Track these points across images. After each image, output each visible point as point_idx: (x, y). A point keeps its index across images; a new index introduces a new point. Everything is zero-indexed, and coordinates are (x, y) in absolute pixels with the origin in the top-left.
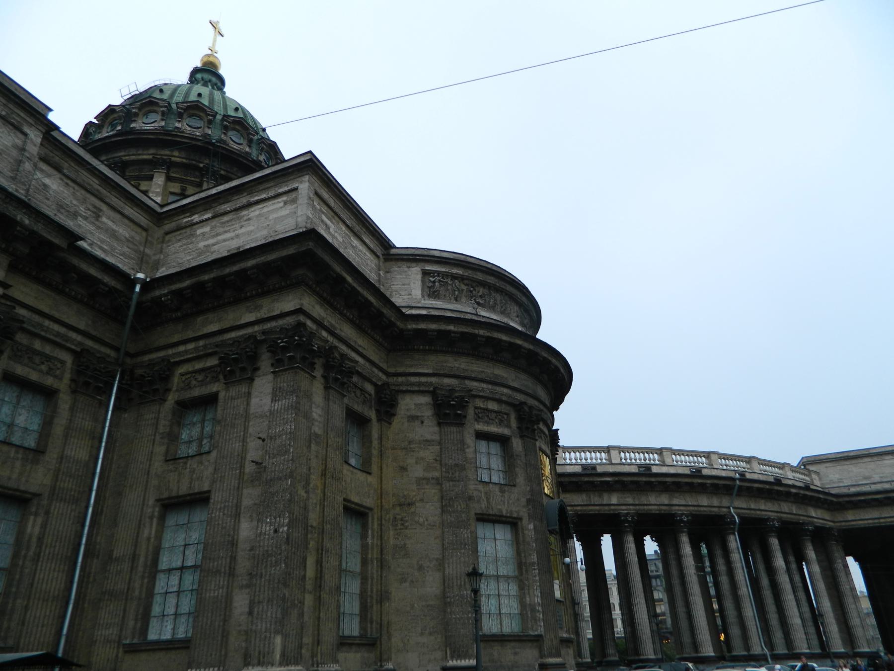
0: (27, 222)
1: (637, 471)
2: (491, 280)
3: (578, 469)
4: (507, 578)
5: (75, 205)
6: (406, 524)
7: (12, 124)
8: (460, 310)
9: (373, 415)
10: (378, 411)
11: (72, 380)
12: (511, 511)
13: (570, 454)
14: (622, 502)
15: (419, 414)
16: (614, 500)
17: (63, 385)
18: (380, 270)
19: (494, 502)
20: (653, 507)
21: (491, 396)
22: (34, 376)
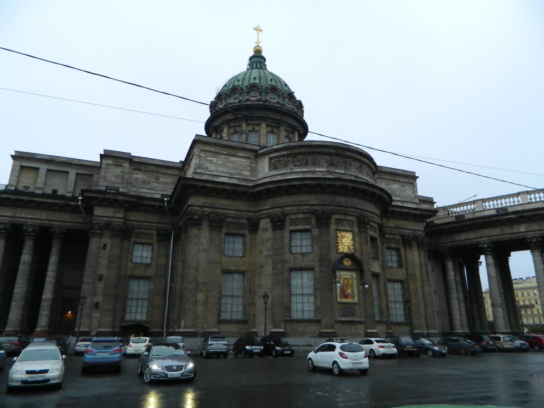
0: (122, 198)
2: (303, 150)
3: (493, 212)
4: (308, 295)
5: (149, 180)
6: (261, 275)
7: (119, 165)
9: (246, 232)
11: (157, 239)
14: (529, 229)
15: (266, 227)
16: (523, 228)
17: (154, 241)
18: (252, 164)
19: (298, 262)
21: (298, 212)
22: (144, 241)
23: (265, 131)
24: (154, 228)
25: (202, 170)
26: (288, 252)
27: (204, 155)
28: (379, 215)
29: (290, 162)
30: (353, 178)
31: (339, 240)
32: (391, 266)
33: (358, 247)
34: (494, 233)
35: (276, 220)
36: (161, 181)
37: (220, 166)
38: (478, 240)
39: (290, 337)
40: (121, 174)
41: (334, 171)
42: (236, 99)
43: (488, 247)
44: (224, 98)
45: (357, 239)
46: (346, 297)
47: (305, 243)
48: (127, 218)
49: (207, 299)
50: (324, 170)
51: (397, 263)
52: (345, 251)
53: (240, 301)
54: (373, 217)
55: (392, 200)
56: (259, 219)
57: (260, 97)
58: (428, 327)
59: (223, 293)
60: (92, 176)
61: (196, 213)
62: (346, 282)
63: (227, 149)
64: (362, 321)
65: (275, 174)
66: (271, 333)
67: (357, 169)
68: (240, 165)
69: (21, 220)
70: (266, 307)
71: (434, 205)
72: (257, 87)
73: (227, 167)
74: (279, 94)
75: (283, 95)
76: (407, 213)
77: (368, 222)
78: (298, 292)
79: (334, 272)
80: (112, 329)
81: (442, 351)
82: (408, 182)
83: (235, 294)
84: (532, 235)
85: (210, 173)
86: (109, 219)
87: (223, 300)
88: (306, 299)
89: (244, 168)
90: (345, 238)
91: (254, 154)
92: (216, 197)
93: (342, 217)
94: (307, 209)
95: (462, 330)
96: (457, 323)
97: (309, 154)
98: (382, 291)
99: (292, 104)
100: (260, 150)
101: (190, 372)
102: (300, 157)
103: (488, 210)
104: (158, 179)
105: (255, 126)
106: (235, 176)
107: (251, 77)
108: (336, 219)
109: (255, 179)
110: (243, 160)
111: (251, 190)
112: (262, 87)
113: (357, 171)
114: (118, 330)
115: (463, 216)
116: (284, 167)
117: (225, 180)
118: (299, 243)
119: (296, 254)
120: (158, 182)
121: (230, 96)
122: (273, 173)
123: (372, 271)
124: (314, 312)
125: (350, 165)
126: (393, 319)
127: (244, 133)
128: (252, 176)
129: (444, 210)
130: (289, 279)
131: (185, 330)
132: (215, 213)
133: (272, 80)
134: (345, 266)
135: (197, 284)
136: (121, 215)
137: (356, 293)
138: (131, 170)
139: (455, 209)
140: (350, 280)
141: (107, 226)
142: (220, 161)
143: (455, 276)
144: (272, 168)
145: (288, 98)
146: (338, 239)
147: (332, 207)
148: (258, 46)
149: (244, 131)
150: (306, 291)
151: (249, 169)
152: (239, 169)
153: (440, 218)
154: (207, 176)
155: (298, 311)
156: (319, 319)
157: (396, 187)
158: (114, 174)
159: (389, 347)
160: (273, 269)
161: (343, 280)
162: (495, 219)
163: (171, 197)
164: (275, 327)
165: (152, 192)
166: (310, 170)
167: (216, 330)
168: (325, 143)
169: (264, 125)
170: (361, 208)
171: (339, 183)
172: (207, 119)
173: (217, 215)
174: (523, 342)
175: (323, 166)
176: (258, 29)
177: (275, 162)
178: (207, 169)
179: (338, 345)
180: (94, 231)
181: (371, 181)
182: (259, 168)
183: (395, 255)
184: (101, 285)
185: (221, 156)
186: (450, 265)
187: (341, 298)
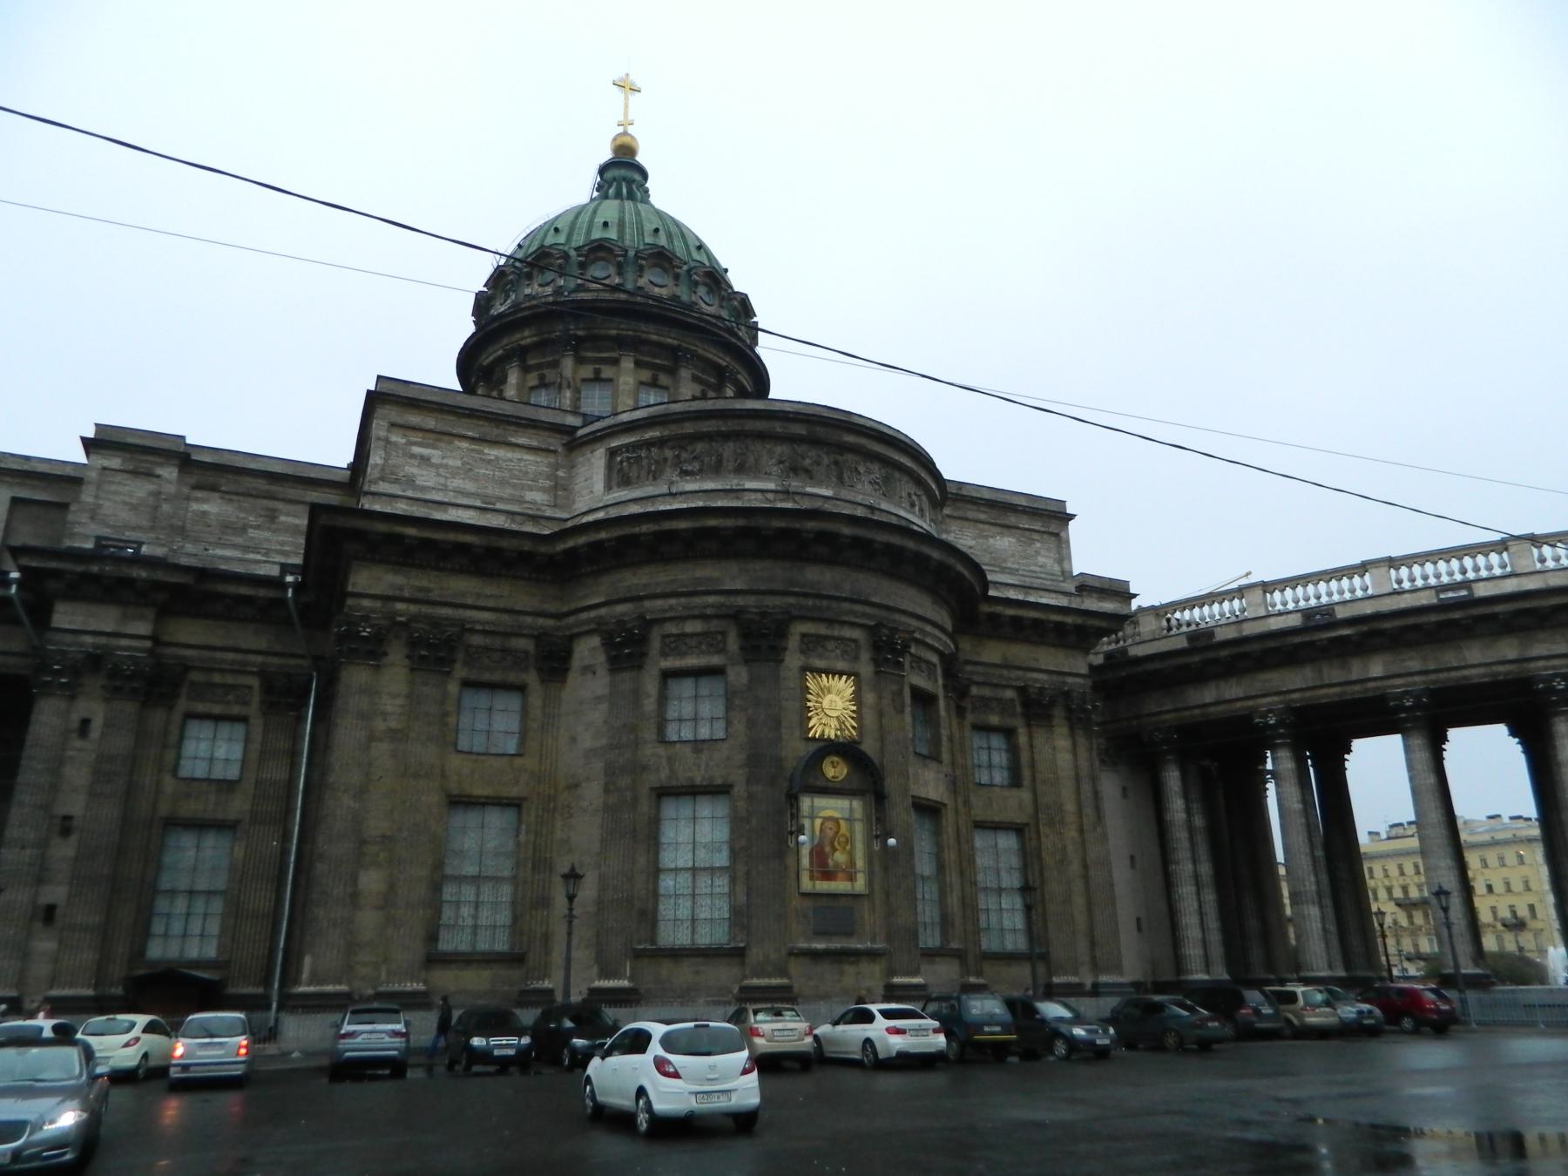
1: (1435, 601)
3: (1295, 621)
4: (712, 870)
5: (243, 518)
6: (572, 811)
7: (143, 473)
8: (652, 494)
9: (532, 678)
10: (540, 670)
11: (262, 702)
13: (1283, 595)
14: (1395, 669)
17: (253, 709)
19: (681, 767)
20: (1473, 672)
21: (685, 613)
22: (217, 709)
23: (631, 380)
24: (255, 669)
25: (393, 486)
26: (654, 737)
27: (404, 441)
28: (950, 628)
29: (669, 463)
30: (860, 512)
31: (810, 701)
32: (989, 783)
33: (870, 719)
34: (1296, 682)
35: (619, 639)
36: (283, 523)
37: (454, 473)
38: (1251, 703)
39: (527, 1008)
40: (151, 500)
41: (800, 490)
42: (548, 284)
43: (1280, 724)
44: (511, 282)
45: (869, 698)
46: (828, 875)
47: (706, 709)
48: (166, 638)
49: (392, 887)
50: (771, 486)
51: (1006, 774)
52: (831, 733)
53: (506, 891)
54: (923, 632)
55: (986, 585)
56: (572, 638)
57: (617, 280)
58: (1096, 967)
59: (449, 871)
61: (366, 618)
62: (831, 829)
63: (475, 422)
64: (878, 949)
65: (623, 499)
66: (594, 992)
67: (877, 487)
68: (517, 473)
70: (571, 910)
71: (1130, 604)
72: (610, 251)
73: (476, 480)
74: (678, 270)
75: (690, 276)
76: (1036, 623)
77: (906, 647)
78: (681, 864)
79: (793, 799)
80: (95, 989)
81: (1095, 1041)
82: (1043, 529)
83: (490, 872)
84: (1403, 685)
85: (419, 495)
86: (103, 640)
87: (449, 892)
88: (704, 882)
89: (530, 482)
90: (829, 692)
91: (566, 439)
92: (437, 569)
93: (822, 630)
94: (713, 606)
95: (1208, 972)
96: (1192, 952)
97: (726, 436)
98: (951, 856)
99: (717, 302)
101: (59, 1142)
102: (700, 447)
103: (1280, 614)
104: (272, 516)
105: (602, 367)
106: (499, 506)
107: (596, 220)
108: (804, 635)
109: (565, 515)
110: (529, 457)
111: (543, 549)
112: (627, 251)
113: (875, 490)
114: (118, 991)
115: (1209, 633)
116: (651, 477)
117: (469, 519)
118: (687, 709)
119: (678, 745)
120: (274, 526)
121: (529, 277)
122: (616, 495)
123: (915, 794)
124: (726, 925)
125: (854, 474)
126: (989, 943)
127: (569, 387)
128: (555, 506)
129: (1157, 615)
130: (655, 823)
131: (312, 989)
132: (427, 617)
133: (657, 230)
134: (827, 779)
135: (363, 842)
136: (143, 628)
138: (186, 490)
139: (1187, 615)
140: (842, 823)
141: (95, 661)
142: (454, 458)
143: (1188, 810)
144: (614, 483)
145: (705, 284)
146: (809, 696)
147: (791, 600)
148: (625, 133)
149: (566, 379)
151: (548, 483)
152: (514, 486)
153: (1147, 639)
154: (407, 504)
155: (678, 923)
156: (742, 945)
157: (1007, 544)
158: (127, 499)
159: (920, 1033)
160: (606, 791)
161: (822, 824)
162: (1297, 640)
163: (303, 569)
164: (605, 973)
165: (251, 556)
166: (728, 487)
167: (421, 987)
168: (777, 404)
169: (628, 364)
170: (885, 602)
171: (811, 525)
172: (462, 345)
173: (435, 623)
174: (1366, 1007)
175: (770, 474)
176: (627, 87)
177: (625, 464)
178: (410, 482)
179: (657, 1030)
180: (49, 679)
181: (922, 523)
182: (578, 481)
183: (1000, 749)
184: (64, 851)
185: (457, 443)
186: (1173, 779)
187: (812, 878)
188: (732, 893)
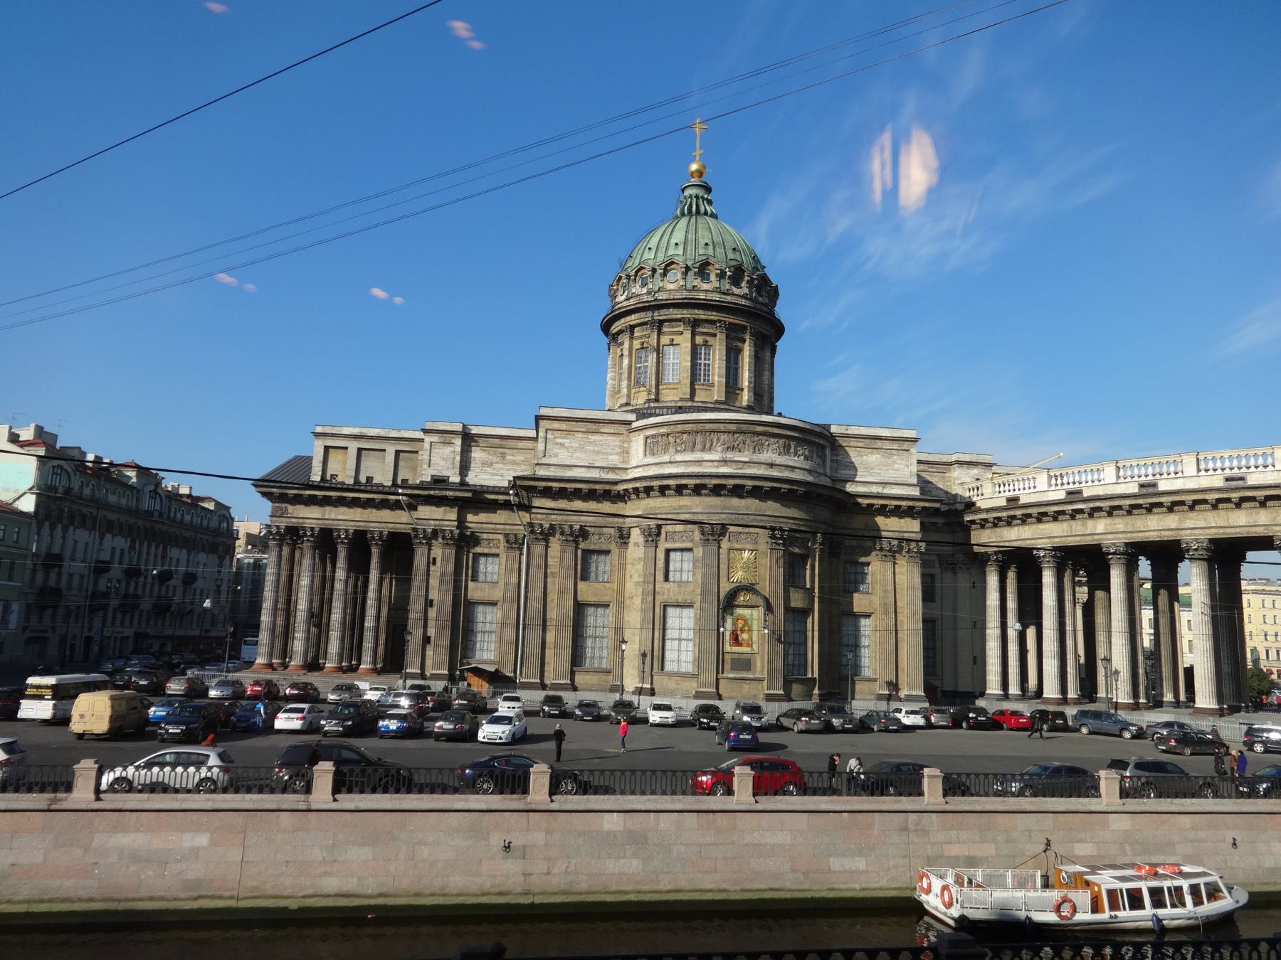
9: (613, 547)
12: (686, 600)
14: (1110, 529)
20: (1151, 534)
57: (682, 283)
60: (417, 452)
69: (331, 522)
73: (586, 452)
86: (438, 522)
100: (637, 420)
102: (685, 436)
104: (503, 456)
110: (610, 438)
133: (707, 244)
137: (755, 639)
147: (723, 516)
150: (684, 635)
151: (618, 450)
188: (694, 651)
